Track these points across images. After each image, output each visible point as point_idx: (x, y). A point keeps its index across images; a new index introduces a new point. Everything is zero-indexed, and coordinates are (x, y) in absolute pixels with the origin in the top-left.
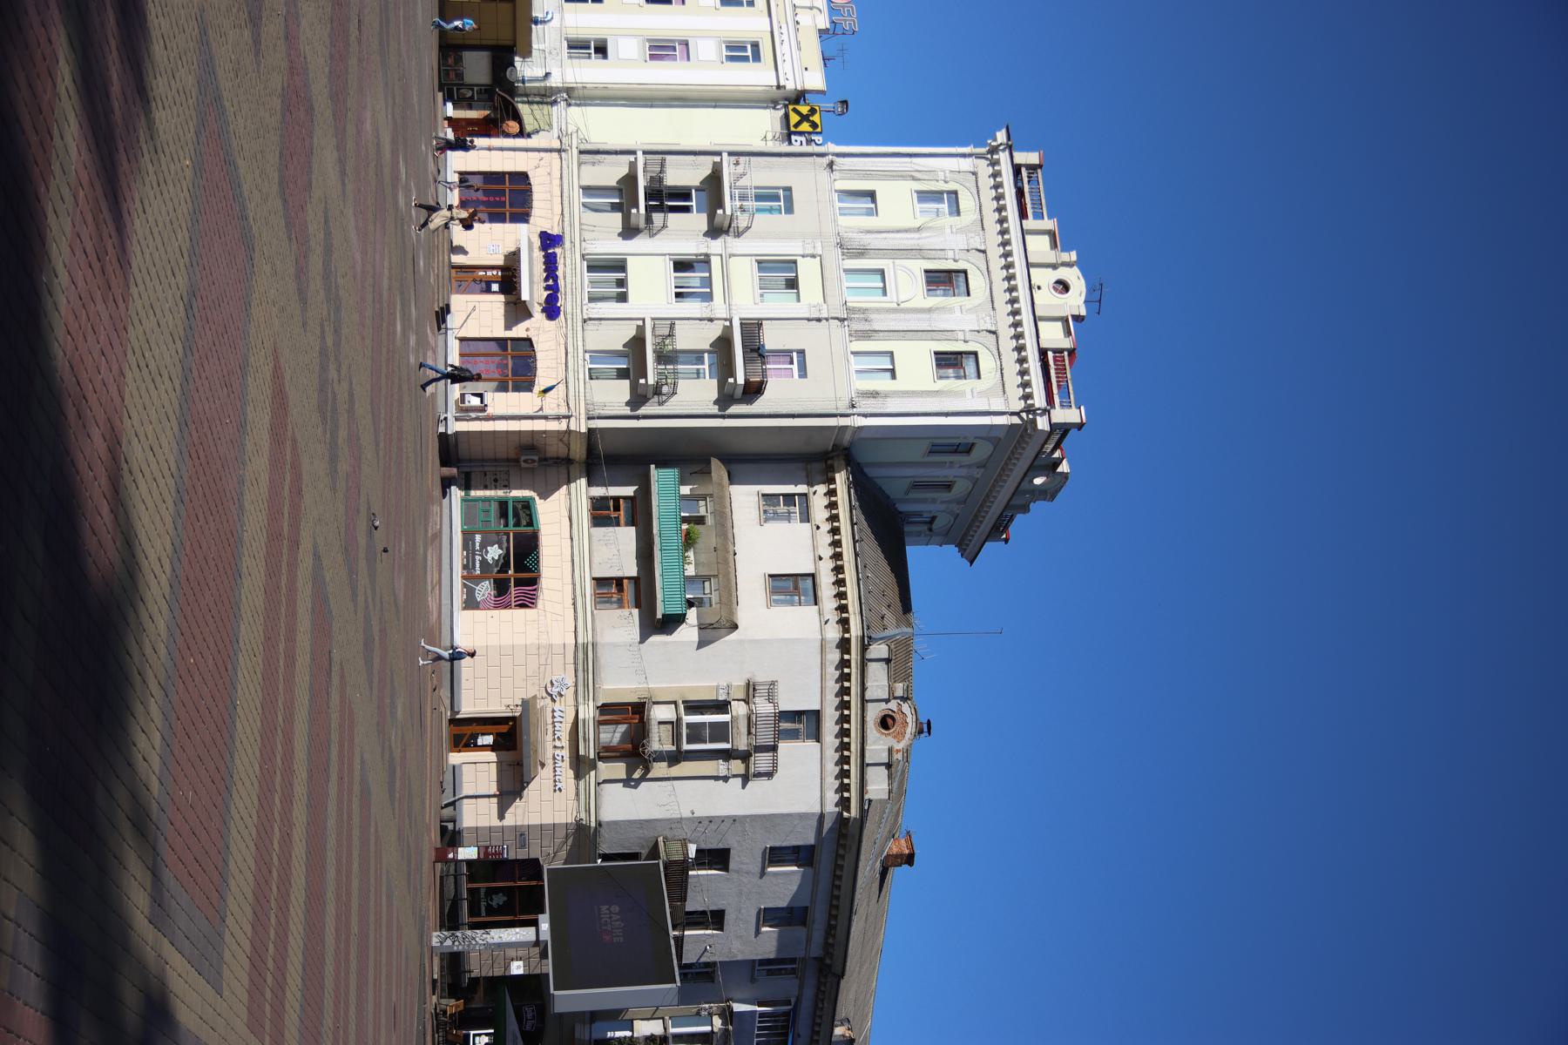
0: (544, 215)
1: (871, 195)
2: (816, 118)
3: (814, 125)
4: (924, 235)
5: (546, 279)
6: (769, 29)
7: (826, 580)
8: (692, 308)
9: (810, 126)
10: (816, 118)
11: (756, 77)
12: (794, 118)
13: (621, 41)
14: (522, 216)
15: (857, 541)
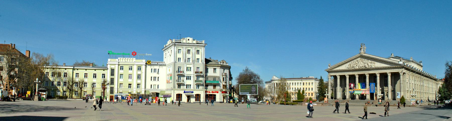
0: (181, 92)
2: (149, 61)
3: (150, 61)
6: (136, 65)
7: (214, 67)
8: (192, 78)
10: (149, 61)
11: (143, 68)
13: (138, 82)
14: (181, 95)
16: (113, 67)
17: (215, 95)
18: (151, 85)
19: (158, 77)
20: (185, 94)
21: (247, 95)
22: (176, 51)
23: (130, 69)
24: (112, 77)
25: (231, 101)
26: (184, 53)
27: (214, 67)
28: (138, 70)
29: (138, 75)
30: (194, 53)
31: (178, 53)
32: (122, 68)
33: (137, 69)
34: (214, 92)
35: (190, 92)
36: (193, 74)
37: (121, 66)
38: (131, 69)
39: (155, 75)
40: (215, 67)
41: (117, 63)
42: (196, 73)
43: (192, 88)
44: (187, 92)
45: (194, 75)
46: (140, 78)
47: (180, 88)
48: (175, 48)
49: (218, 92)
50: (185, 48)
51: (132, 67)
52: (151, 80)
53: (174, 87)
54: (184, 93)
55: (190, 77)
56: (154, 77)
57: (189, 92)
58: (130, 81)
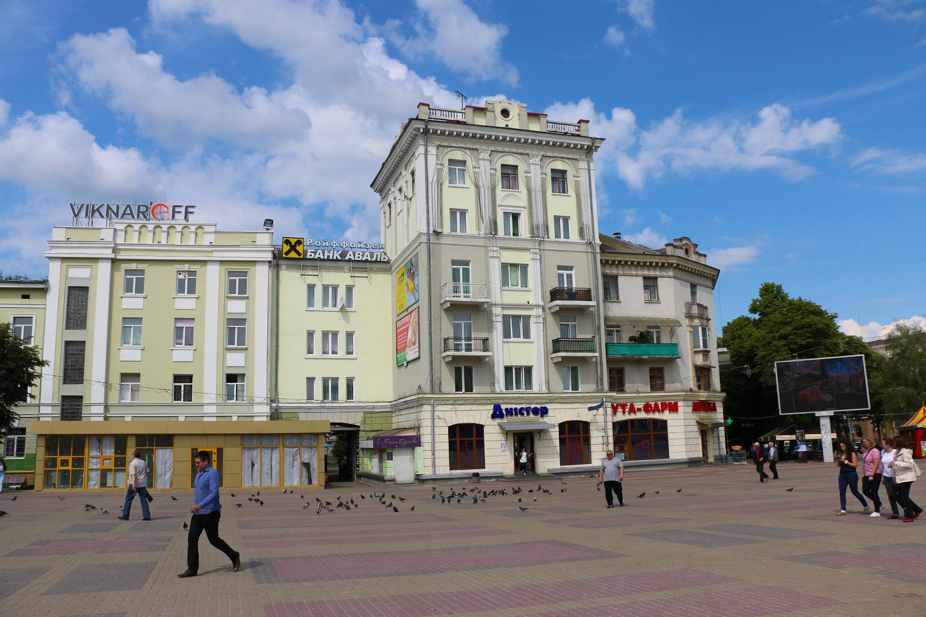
0: (480, 415)
1: (453, 212)
2: (293, 242)
4: (481, 184)
5: (523, 414)
7: (646, 273)
8: (536, 329)
9: (299, 245)
10: (293, 242)
11: (261, 277)
12: (293, 254)
14: (480, 428)
15: (644, 253)
16: (79, 274)
17: (664, 423)
18: (310, 381)
19: (350, 335)
20: (499, 425)
21: (818, 414)
22: (439, 172)
23: (181, 290)
24: (75, 335)
26: (485, 182)
27: (646, 273)
28: (232, 290)
29: (231, 321)
30: (536, 184)
31: (446, 184)
32: (135, 284)
33: (225, 287)
34: (656, 405)
35: (528, 410)
36: (537, 306)
37: (128, 272)
38: (192, 290)
39: (329, 320)
40: (652, 273)
41: (109, 253)
42: (555, 294)
43: (540, 385)
44: (509, 412)
45: (544, 309)
46: (242, 341)
47: (469, 389)
49: (674, 408)
50: (487, 156)
51: (194, 273)
52: (310, 351)
53: (435, 386)
54: (494, 416)
56: (325, 334)
57: (520, 412)
58: (182, 356)
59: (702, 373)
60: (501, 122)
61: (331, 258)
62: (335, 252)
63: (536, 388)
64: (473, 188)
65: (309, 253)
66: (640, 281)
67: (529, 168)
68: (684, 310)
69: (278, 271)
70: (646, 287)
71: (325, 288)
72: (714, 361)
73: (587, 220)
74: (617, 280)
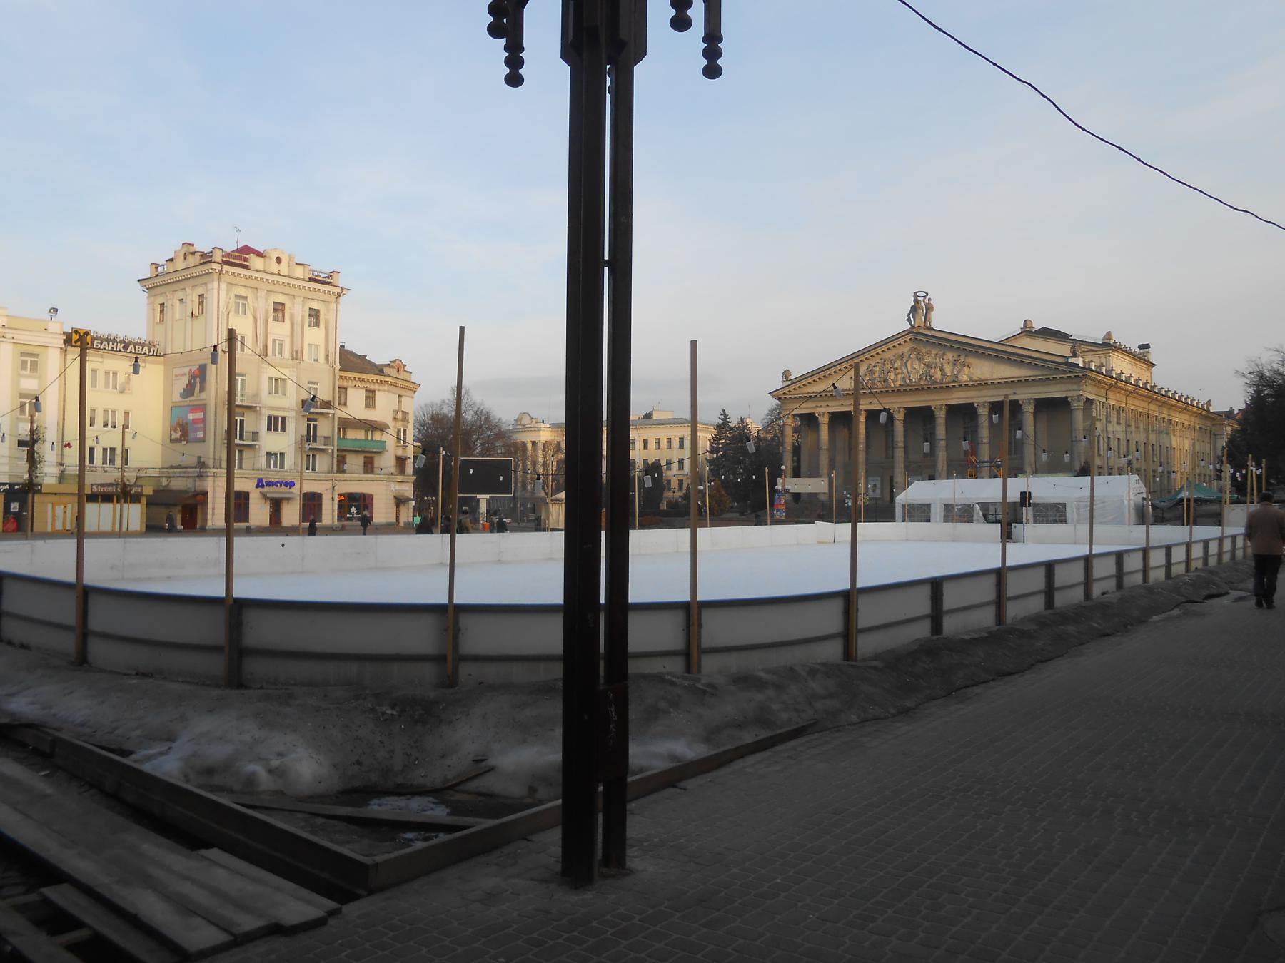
8: (290, 426)
20: (260, 492)
25: (1129, 627)
26: (261, 315)
44: (268, 484)
48: (223, 286)
55: (283, 419)
56: (106, 411)
57: (274, 484)
59: (401, 461)
60: (274, 267)
61: (115, 349)
62: (119, 344)
63: (286, 467)
64: (251, 319)
65: (95, 344)
66: (363, 393)
67: (294, 306)
68: (391, 415)
69: (66, 355)
70: (367, 397)
71: (107, 373)
72: (410, 452)
73: (331, 349)
74: (346, 390)
